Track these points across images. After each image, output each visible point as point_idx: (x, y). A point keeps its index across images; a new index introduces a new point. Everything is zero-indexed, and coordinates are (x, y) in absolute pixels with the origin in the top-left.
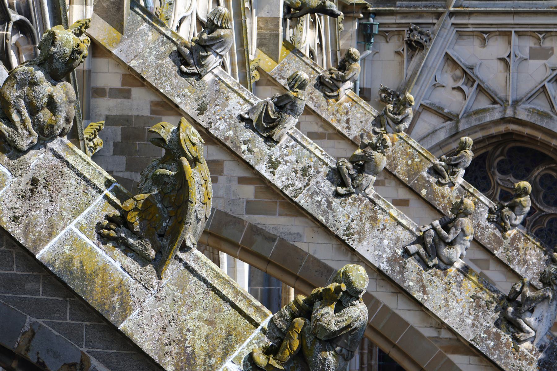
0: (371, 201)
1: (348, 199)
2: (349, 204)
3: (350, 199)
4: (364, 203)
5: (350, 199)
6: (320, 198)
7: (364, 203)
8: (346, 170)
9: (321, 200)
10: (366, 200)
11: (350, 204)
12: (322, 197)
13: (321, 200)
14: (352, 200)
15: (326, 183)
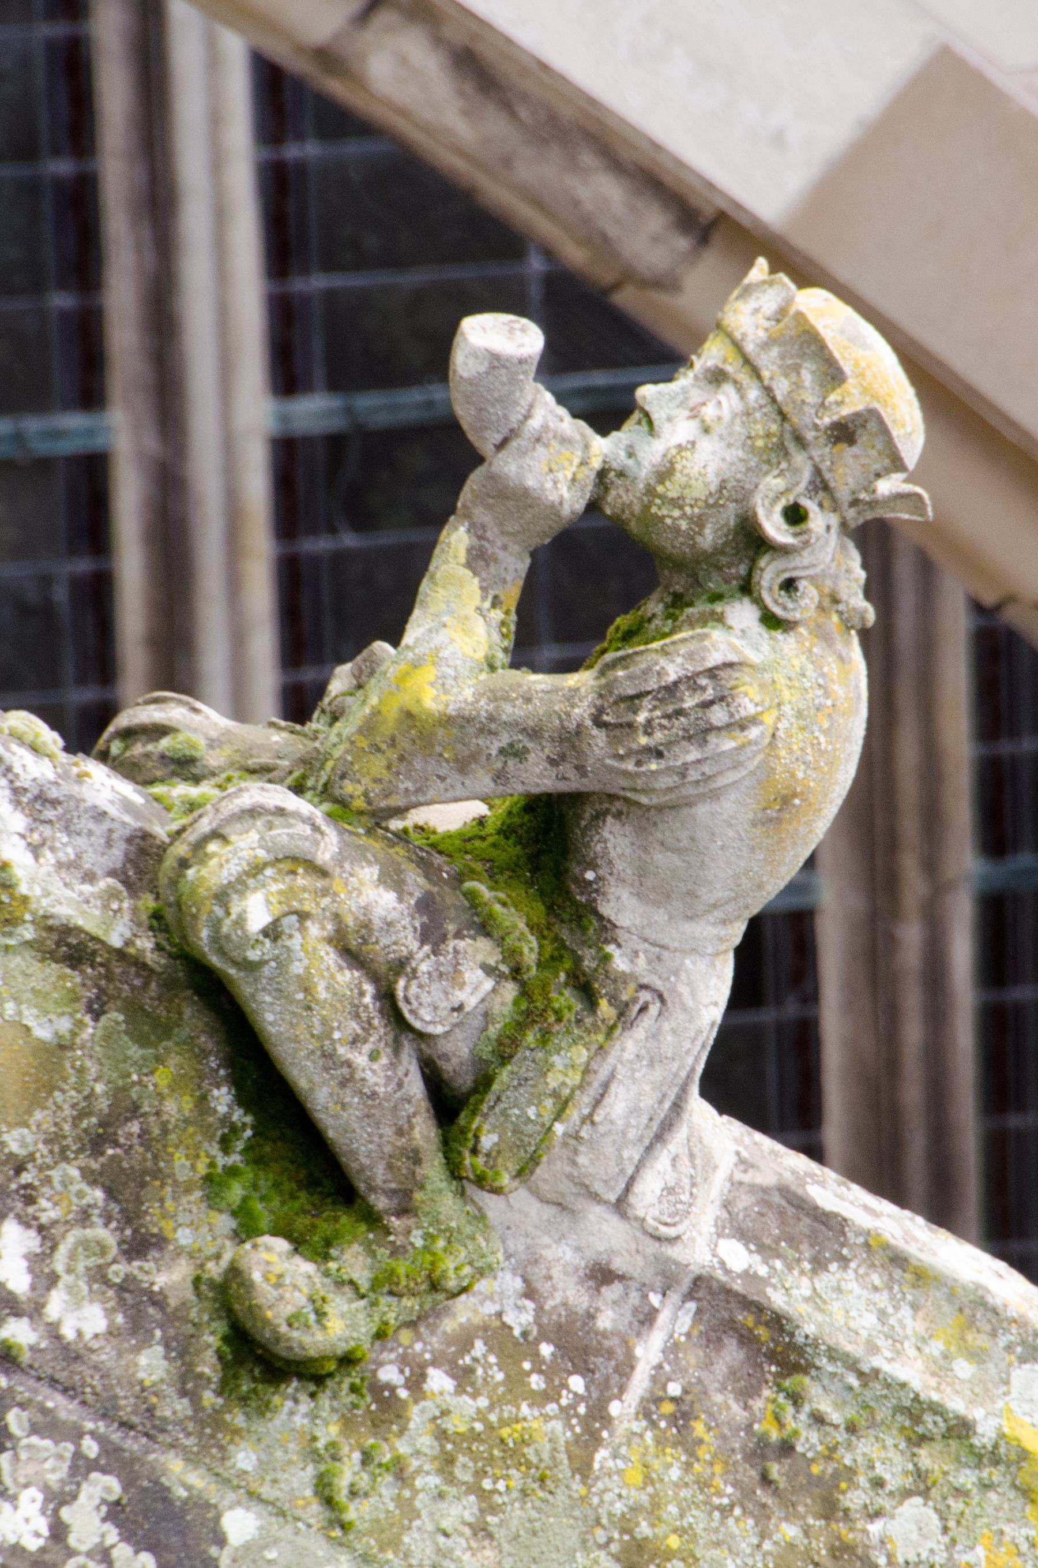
0: (731, 1326)
1: (416, 1383)
2: (447, 1462)
3: (438, 1381)
4: (639, 1384)
5: (438, 1381)
6: (31, 1500)
7: (639, 1384)
8: (347, 977)
9: (58, 1532)
10: (647, 1318)
11: (464, 1471)
12: (56, 1473)
13: (58, 1532)
14: (463, 1377)
15: (48, 1211)
